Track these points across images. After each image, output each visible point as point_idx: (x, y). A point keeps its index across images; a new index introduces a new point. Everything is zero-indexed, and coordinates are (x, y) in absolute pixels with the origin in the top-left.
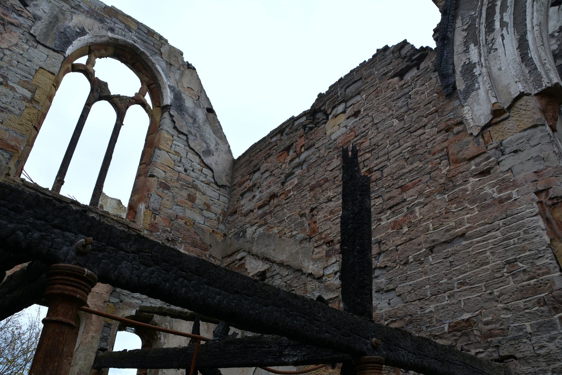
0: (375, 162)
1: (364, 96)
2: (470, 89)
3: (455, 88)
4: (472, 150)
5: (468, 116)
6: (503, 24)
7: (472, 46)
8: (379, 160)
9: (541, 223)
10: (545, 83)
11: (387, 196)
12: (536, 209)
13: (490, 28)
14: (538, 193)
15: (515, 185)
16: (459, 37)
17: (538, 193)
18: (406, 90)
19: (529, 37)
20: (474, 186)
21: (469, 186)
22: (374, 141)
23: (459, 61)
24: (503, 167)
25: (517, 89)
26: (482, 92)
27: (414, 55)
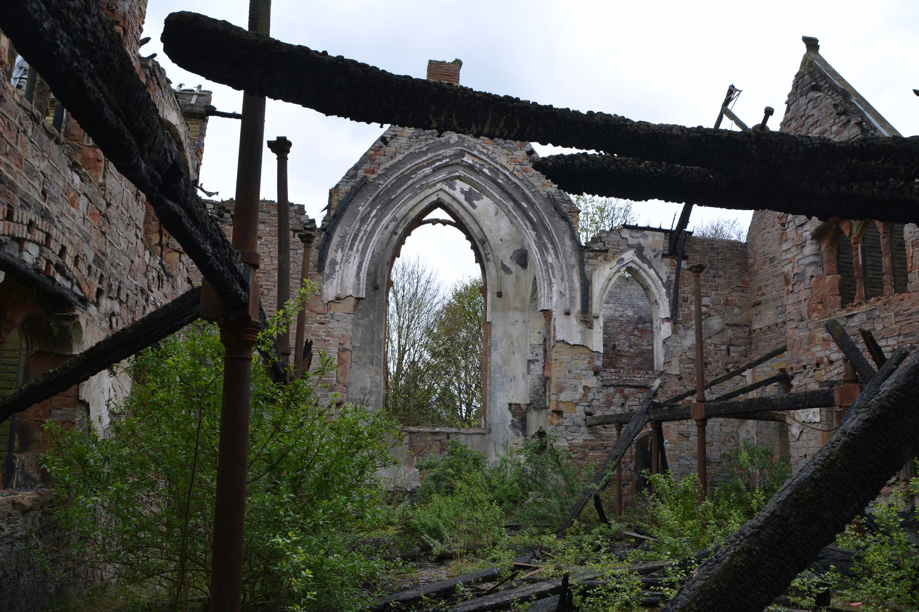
0: (266, 283)
1: (268, 229)
2: (330, 276)
3: (323, 269)
4: (320, 309)
5: (325, 291)
6: (357, 250)
7: (340, 250)
8: (269, 283)
9: (337, 357)
10: (360, 296)
11: (270, 309)
12: (337, 351)
13: (351, 249)
14: (340, 344)
15: (333, 336)
16: (335, 240)
17: (340, 344)
18: (296, 247)
19: (364, 264)
20: (316, 328)
21: (313, 326)
22: (268, 268)
23: (331, 255)
24: (330, 325)
25: (350, 292)
26: (335, 281)
27: (307, 224)
